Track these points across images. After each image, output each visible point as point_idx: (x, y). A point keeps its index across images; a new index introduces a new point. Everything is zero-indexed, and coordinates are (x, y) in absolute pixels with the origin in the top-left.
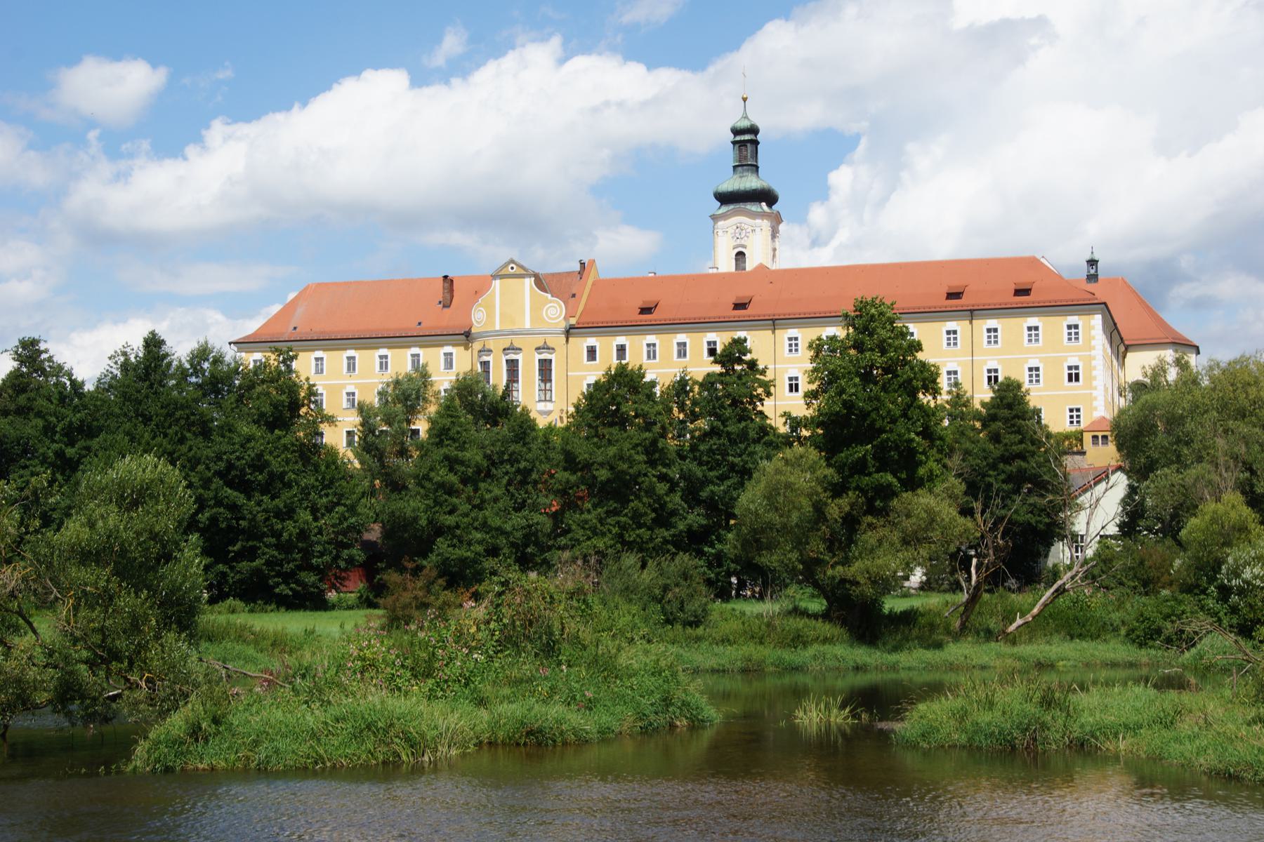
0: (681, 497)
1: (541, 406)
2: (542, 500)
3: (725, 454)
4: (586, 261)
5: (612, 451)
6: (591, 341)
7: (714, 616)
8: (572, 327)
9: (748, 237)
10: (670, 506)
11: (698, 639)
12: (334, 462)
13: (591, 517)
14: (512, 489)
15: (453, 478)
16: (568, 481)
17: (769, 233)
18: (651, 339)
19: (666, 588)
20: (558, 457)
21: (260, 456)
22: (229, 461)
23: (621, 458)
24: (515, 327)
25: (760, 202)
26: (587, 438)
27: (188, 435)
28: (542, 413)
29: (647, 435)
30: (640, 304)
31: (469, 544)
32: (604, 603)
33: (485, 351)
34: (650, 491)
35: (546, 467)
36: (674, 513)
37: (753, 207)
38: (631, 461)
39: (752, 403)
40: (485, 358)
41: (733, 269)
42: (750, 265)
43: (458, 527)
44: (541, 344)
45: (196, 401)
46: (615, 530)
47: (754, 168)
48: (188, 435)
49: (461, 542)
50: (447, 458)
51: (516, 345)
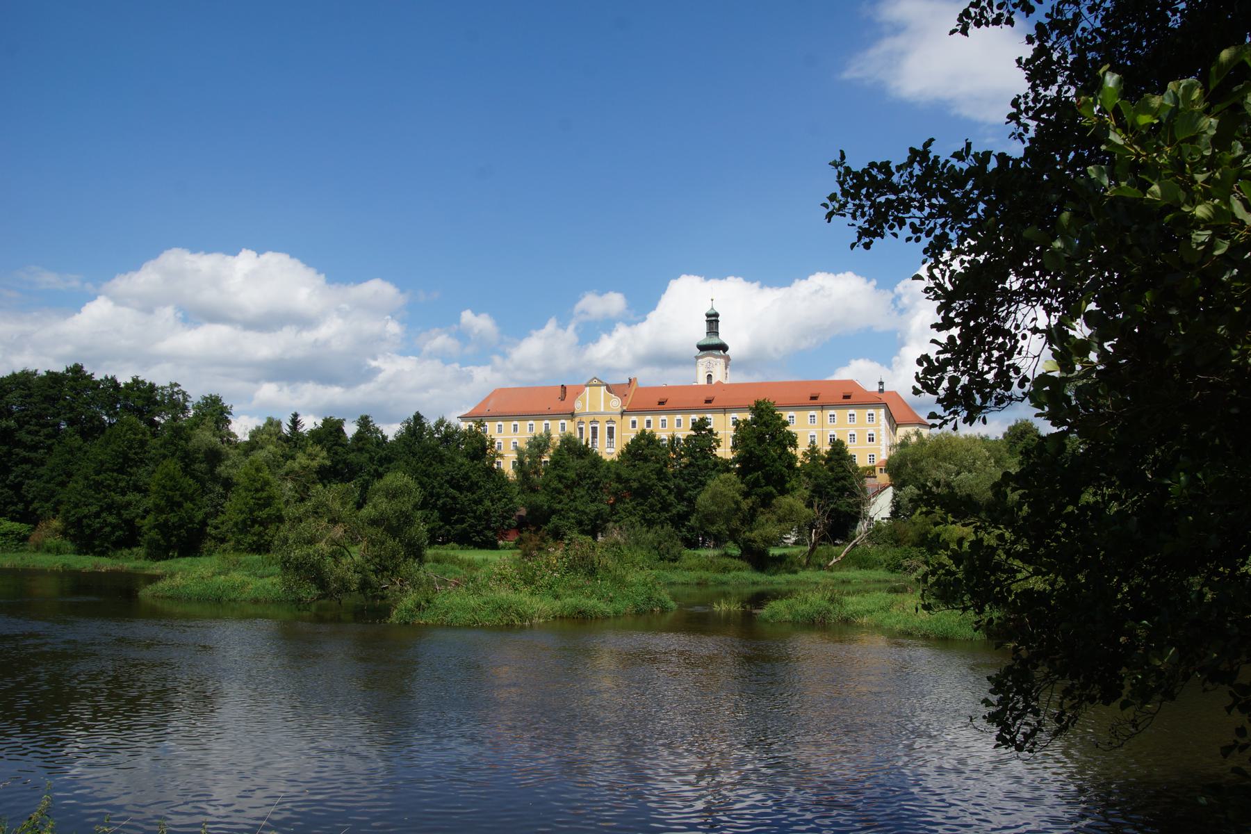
0: (675, 497)
1: (608, 450)
2: (605, 497)
3: (696, 475)
4: (632, 378)
5: (640, 473)
6: (634, 418)
7: (685, 557)
8: (624, 411)
10: (669, 501)
11: (676, 568)
12: (502, 477)
13: (629, 506)
14: (590, 492)
15: (560, 486)
16: (618, 488)
18: (664, 417)
19: (660, 543)
20: (614, 476)
21: (467, 473)
22: (452, 475)
23: (644, 477)
24: (596, 411)
26: (627, 467)
27: (434, 462)
28: (608, 453)
29: (658, 465)
30: (658, 400)
31: (568, 518)
32: (630, 549)
33: (581, 422)
34: (659, 494)
35: (606, 481)
36: (671, 505)
37: (716, 353)
38: (649, 478)
39: (710, 450)
40: (581, 426)
41: (706, 383)
42: (714, 381)
43: (562, 510)
44: (609, 419)
45: (438, 446)
46: (641, 513)
48: (434, 462)
49: (564, 517)
50: (558, 476)
51: (597, 420)
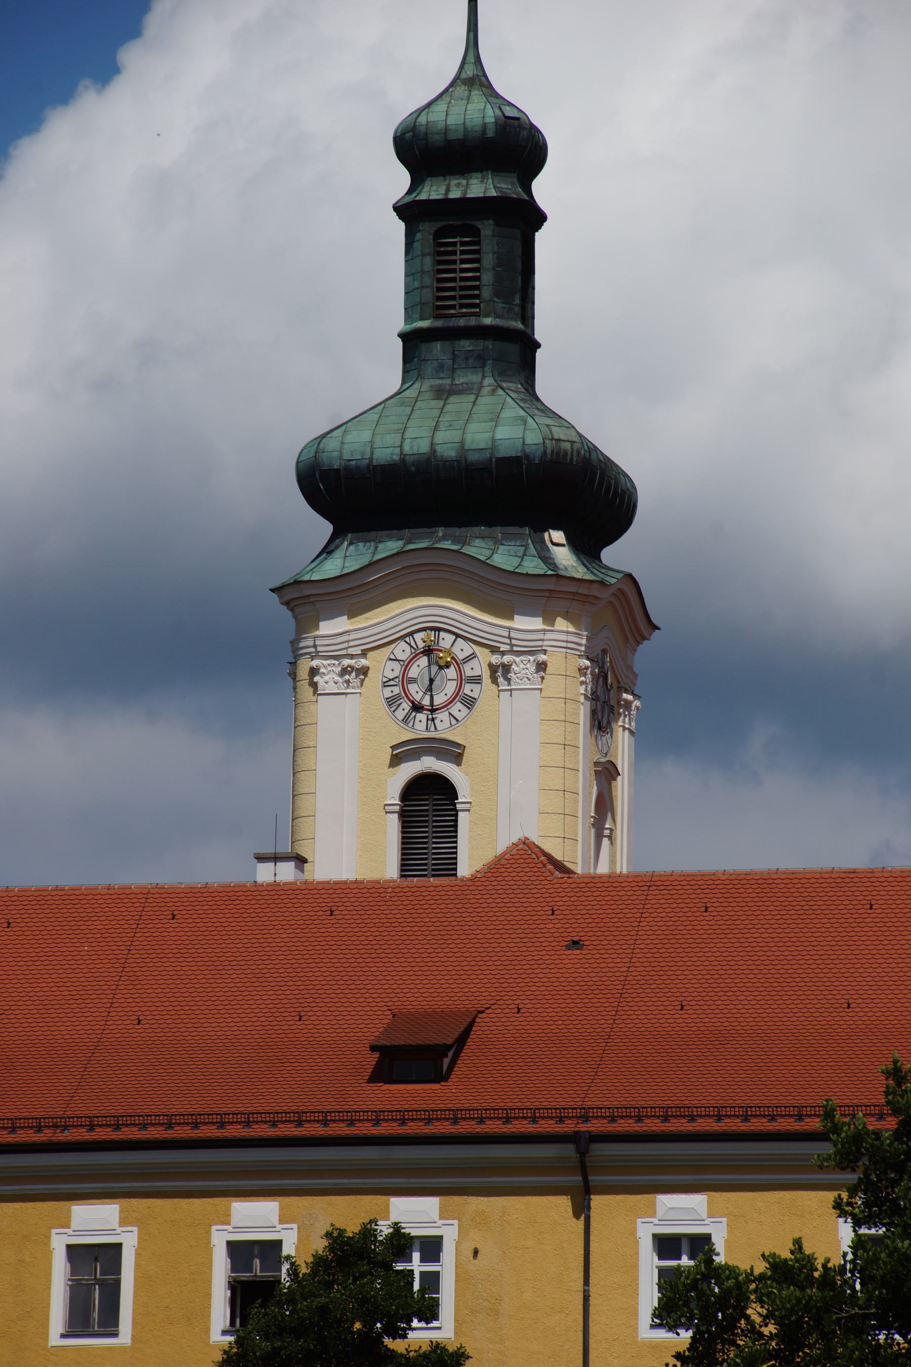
9: (470, 703)
17: (580, 690)
25: (540, 527)
41: (390, 869)
47: (513, 350)
